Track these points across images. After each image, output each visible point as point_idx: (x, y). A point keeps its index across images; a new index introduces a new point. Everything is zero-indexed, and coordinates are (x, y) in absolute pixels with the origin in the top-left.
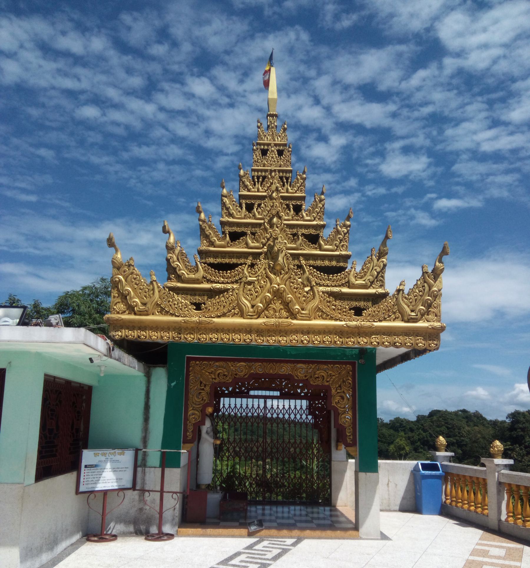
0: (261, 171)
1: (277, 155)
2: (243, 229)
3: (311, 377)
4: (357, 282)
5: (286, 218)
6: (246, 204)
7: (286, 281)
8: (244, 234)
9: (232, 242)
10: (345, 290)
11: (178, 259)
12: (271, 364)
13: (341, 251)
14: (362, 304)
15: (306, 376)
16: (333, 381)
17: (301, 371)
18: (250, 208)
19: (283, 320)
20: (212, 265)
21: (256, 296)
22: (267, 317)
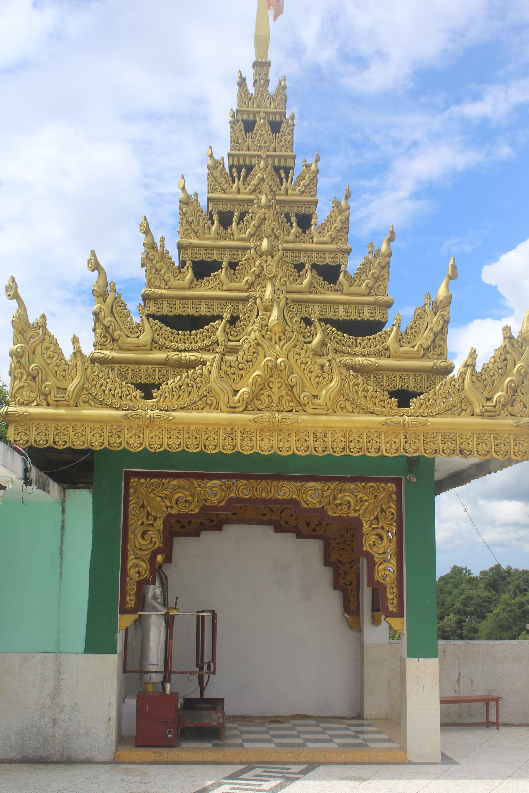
0: (245, 156)
1: (270, 132)
2: (215, 256)
3: (330, 503)
4: (402, 349)
5: (287, 238)
6: (220, 213)
7: (289, 351)
8: (216, 266)
9: (197, 280)
10: (383, 362)
11: (112, 312)
12: (264, 482)
13: (377, 295)
14: (411, 385)
15: (320, 503)
16: (365, 510)
17: (312, 495)
18: (225, 220)
19: (284, 414)
20: (165, 320)
21: (242, 376)
22: (259, 410)
